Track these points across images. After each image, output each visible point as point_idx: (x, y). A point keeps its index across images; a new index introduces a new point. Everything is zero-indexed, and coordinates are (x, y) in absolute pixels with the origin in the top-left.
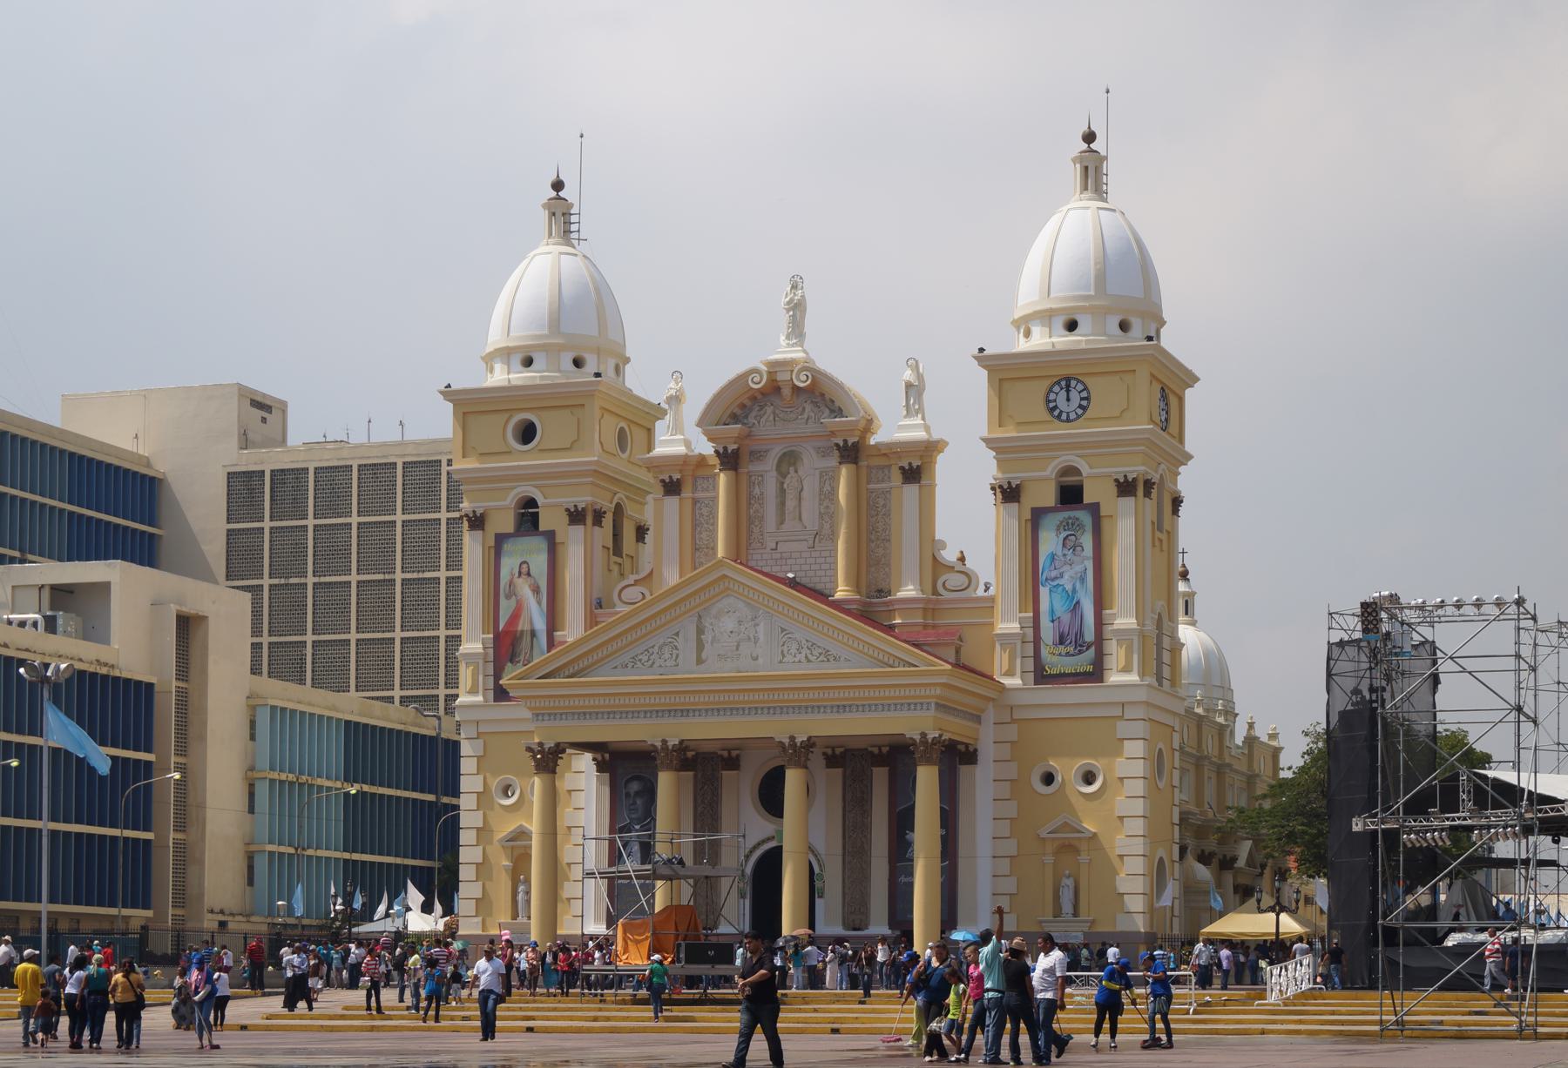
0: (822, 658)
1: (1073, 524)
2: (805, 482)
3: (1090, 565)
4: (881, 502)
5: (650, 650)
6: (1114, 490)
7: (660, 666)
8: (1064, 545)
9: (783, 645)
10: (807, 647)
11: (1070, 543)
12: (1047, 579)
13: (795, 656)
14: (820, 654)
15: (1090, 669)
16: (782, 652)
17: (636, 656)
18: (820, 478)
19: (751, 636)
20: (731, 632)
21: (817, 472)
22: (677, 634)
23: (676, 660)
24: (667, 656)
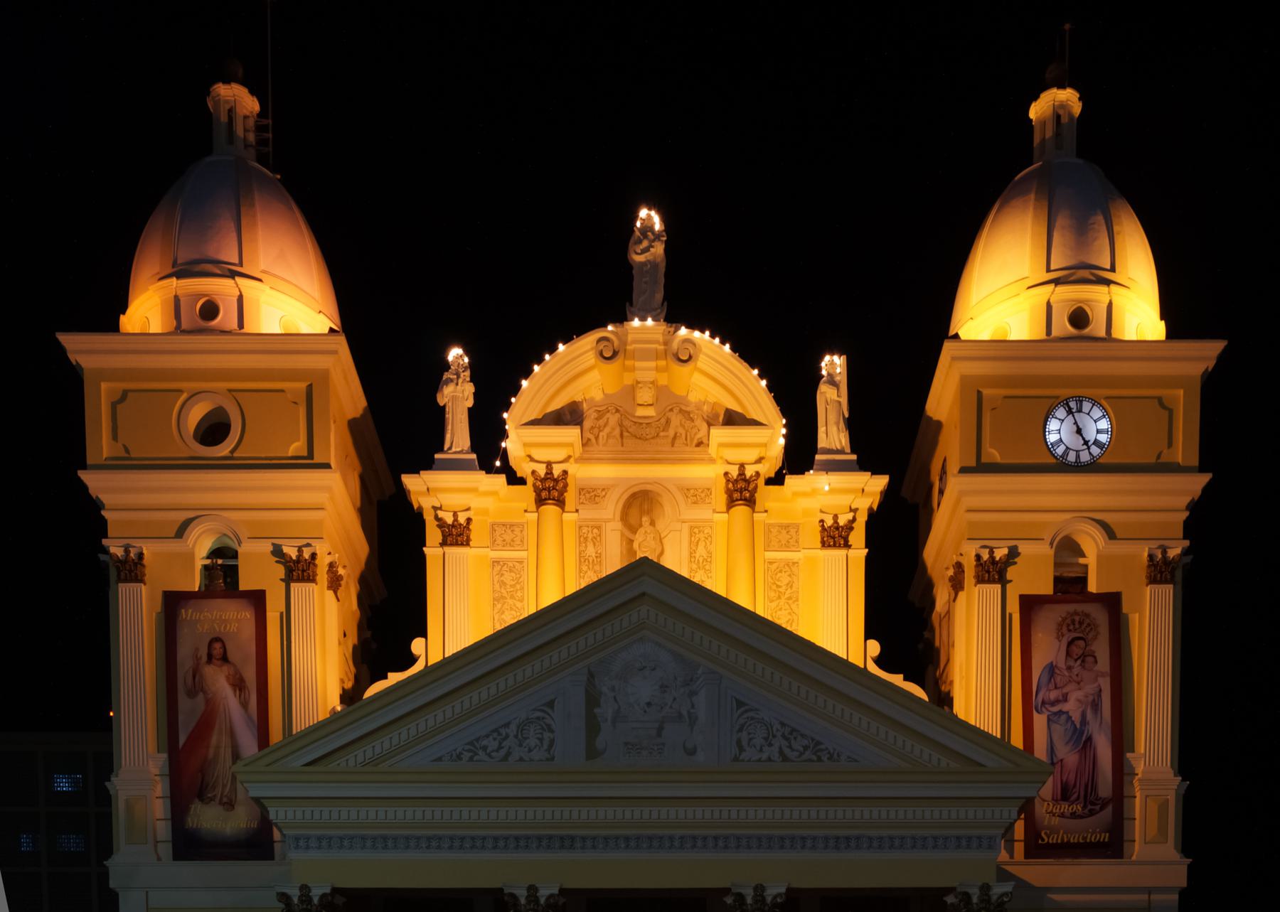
0: (808, 755)
1: (1081, 623)
2: (665, 541)
3: (1105, 684)
4: (785, 579)
5: (503, 731)
6: (1142, 575)
7: (521, 759)
8: (1068, 654)
9: (740, 730)
10: (783, 736)
11: (1077, 651)
12: (1043, 703)
13: (761, 750)
14: (806, 748)
15: (1105, 837)
16: (739, 742)
17: (477, 740)
18: (691, 536)
19: (685, 713)
20: (649, 704)
21: (686, 527)
22: (551, 704)
23: (548, 750)
24: (533, 742)
